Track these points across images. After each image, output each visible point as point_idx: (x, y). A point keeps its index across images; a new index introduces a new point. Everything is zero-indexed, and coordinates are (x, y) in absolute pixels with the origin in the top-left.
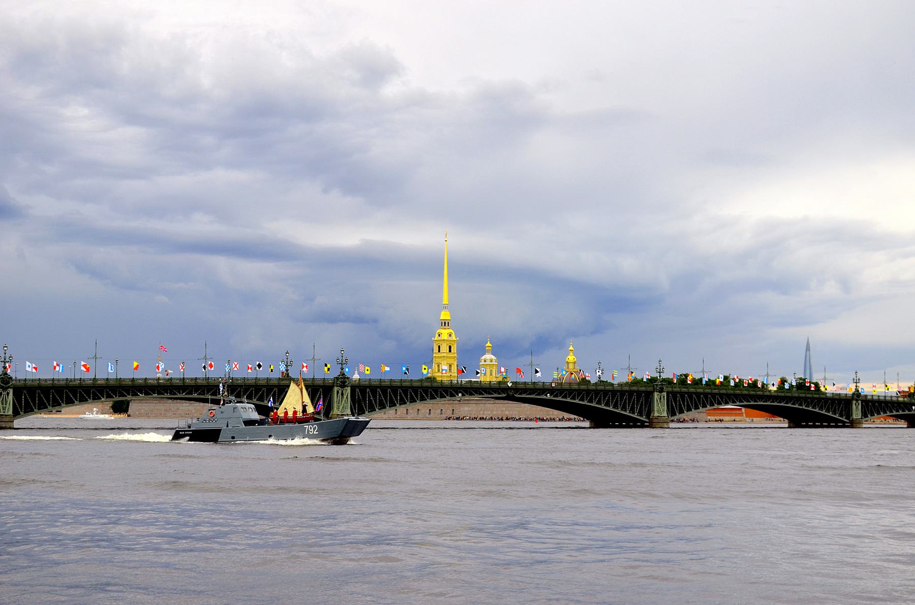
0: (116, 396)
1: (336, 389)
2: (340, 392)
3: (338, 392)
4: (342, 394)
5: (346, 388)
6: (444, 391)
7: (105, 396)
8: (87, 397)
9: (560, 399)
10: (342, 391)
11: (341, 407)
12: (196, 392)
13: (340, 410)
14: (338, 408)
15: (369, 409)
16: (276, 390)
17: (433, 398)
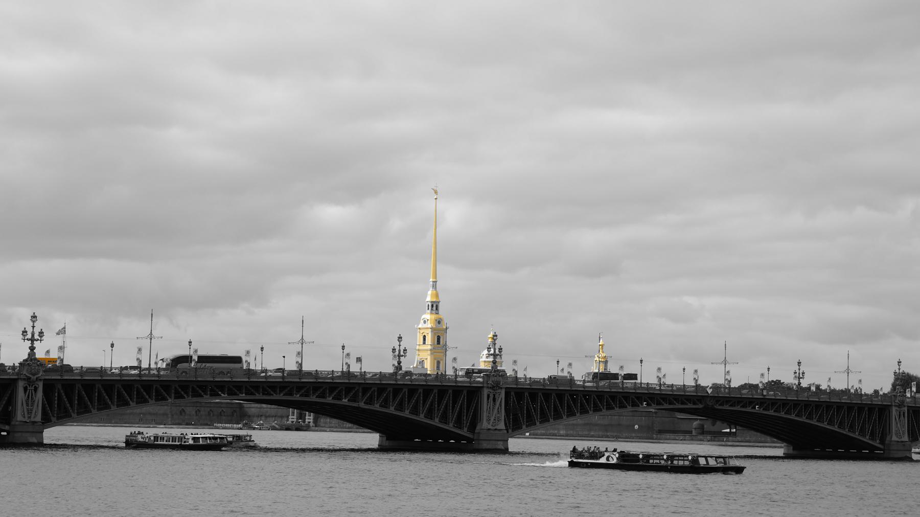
0: (188, 396)
1: (486, 392)
2: (492, 396)
3: (488, 396)
4: (494, 400)
5: (499, 391)
6: (662, 398)
7: (173, 395)
8: (147, 397)
10: (494, 395)
11: (492, 419)
12: (298, 392)
13: (491, 423)
14: (489, 420)
15: (527, 422)
16: (405, 392)
17: (609, 408)
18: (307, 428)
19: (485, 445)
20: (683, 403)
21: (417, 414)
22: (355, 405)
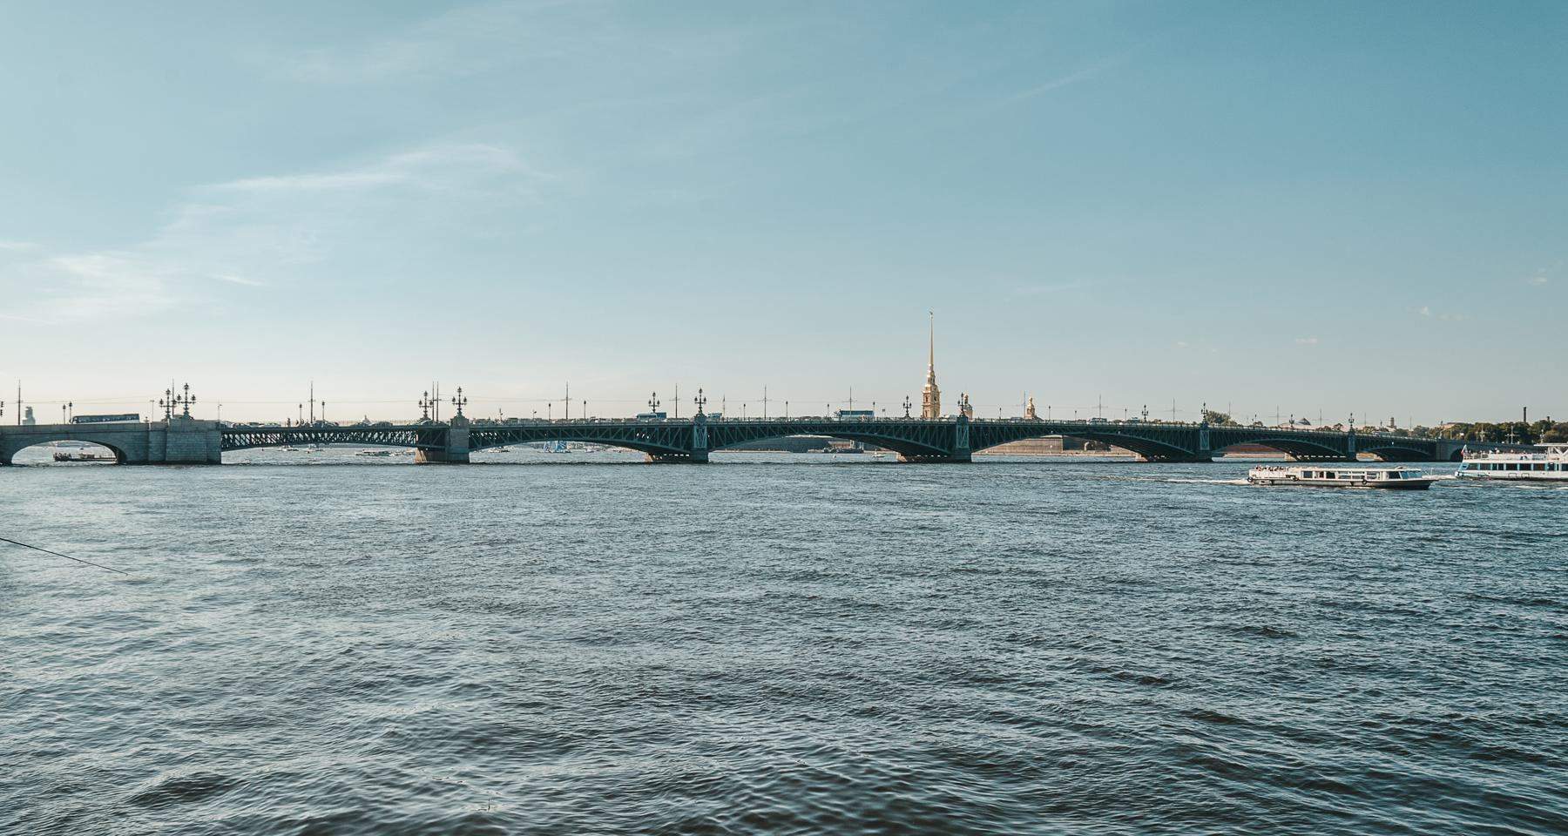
1: (957, 427)
9: (1128, 436)
18: (861, 452)
19: (958, 458)
20: (1074, 431)
21: (918, 441)
22: (881, 436)
